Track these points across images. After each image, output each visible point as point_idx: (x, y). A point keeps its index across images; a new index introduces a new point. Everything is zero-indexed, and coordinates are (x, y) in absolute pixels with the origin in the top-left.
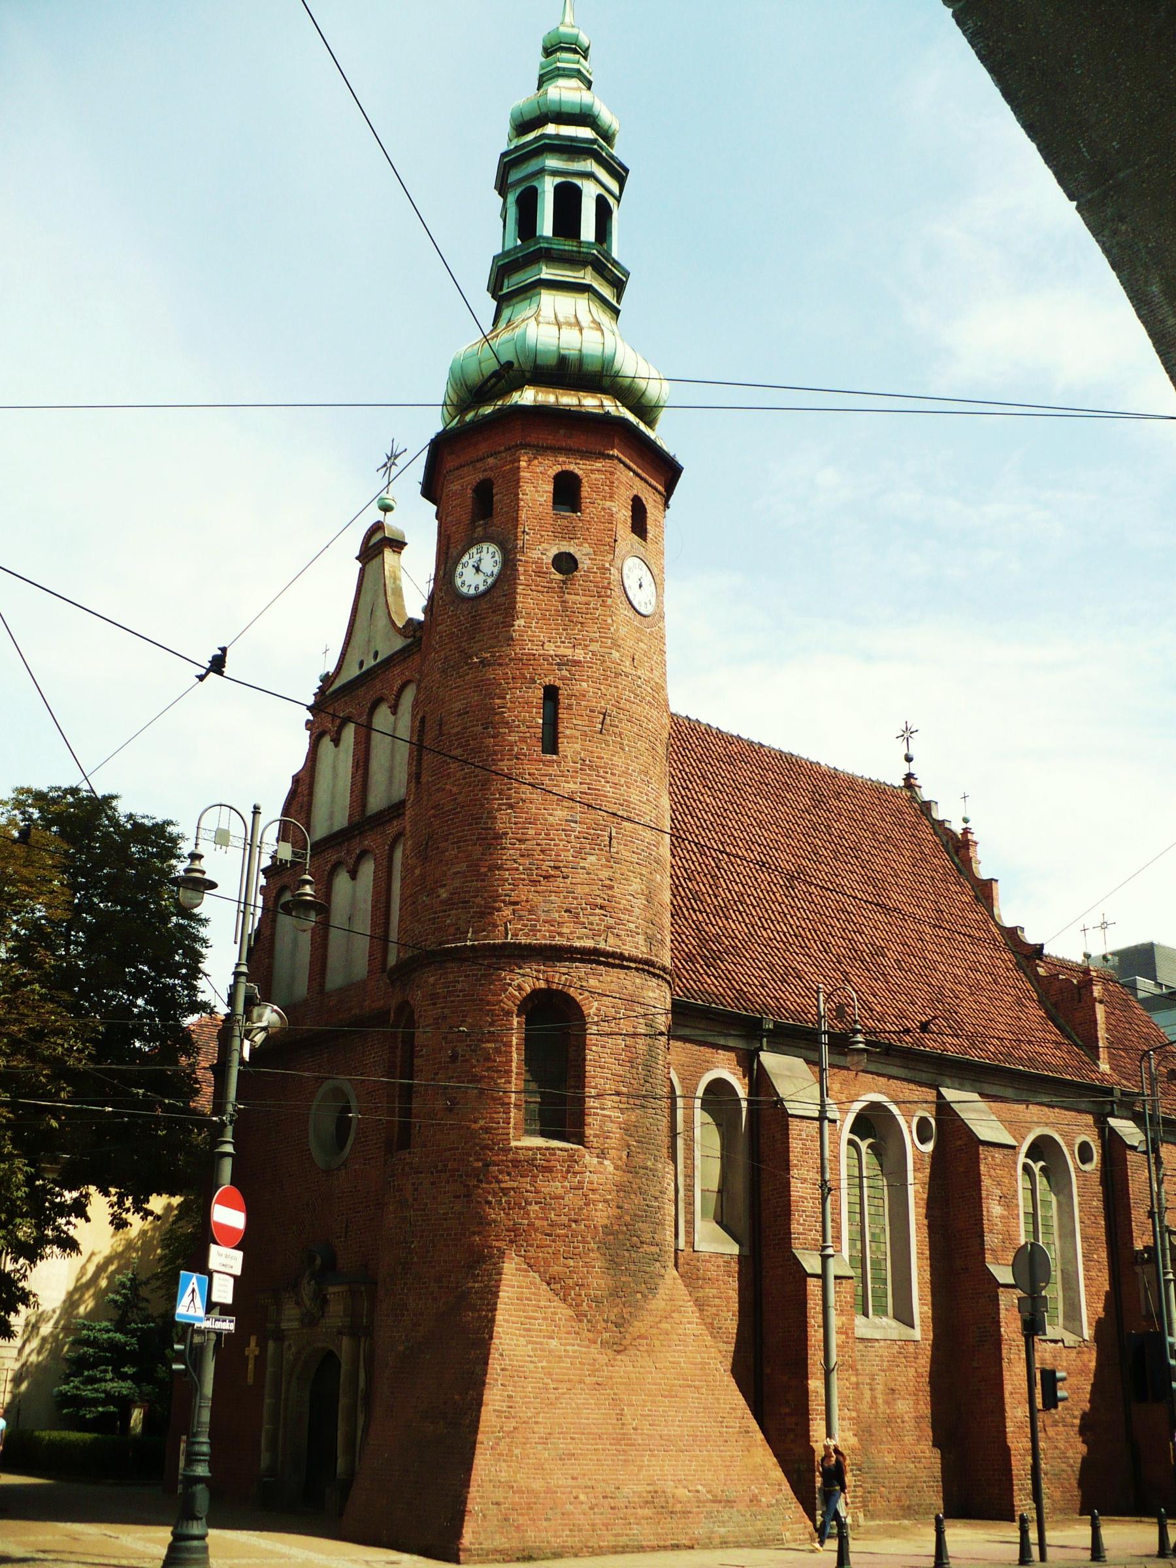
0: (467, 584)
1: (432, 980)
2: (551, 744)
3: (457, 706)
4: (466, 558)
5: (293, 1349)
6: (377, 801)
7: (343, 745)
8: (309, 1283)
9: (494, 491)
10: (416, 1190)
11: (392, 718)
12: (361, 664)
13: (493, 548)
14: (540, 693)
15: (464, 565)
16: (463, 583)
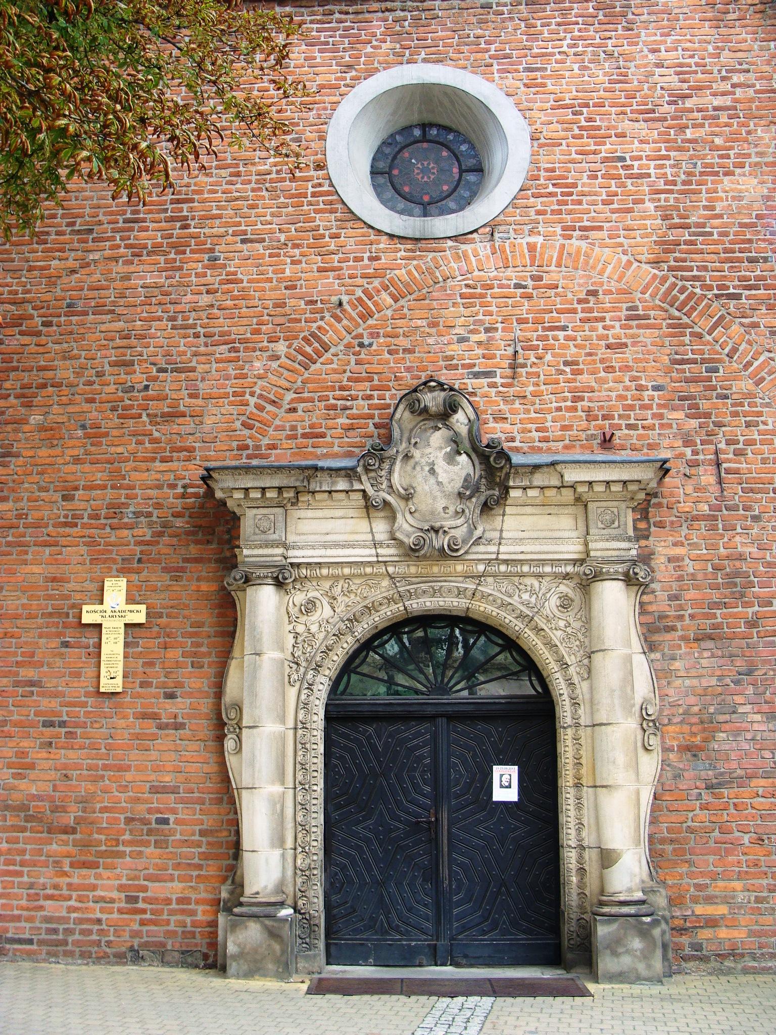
8: (450, 459)
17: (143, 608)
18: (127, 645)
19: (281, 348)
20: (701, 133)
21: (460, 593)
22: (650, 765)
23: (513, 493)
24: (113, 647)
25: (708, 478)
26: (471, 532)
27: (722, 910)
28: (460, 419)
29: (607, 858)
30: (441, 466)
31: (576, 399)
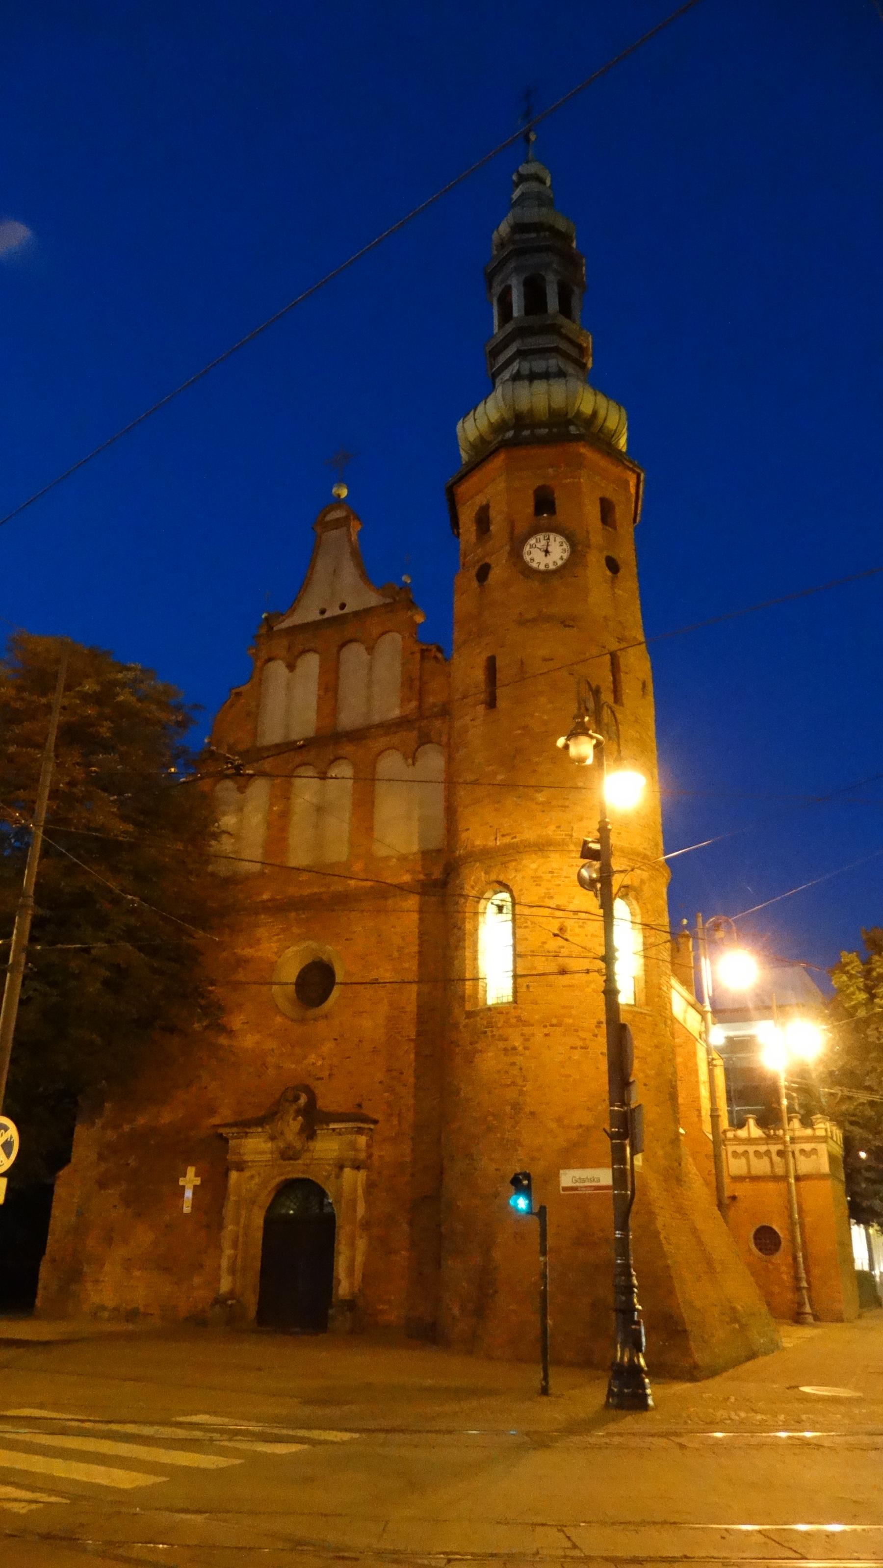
0: (537, 561)
1: (534, 866)
2: (617, 699)
3: (543, 652)
4: (532, 541)
5: (257, 1180)
6: (348, 719)
7: (299, 670)
8: (294, 1119)
9: (555, 495)
10: (527, 1040)
11: (369, 657)
12: (323, 612)
13: (560, 539)
14: (608, 657)
15: (531, 546)
16: (532, 560)
17: (199, 1179)
18: (194, 1194)
19: (251, 1070)
20: (407, 965)
21: (303, 1172)
22: (361, 1244)
23: (319, 1132)
24: (189, 1194)
25: (395, 1122)
26: (303, 1148)
27: (386, 1307)
28: (303, 1100)
29: (339, 1282)
30: (291, 1122)
31: (352, 1088)
